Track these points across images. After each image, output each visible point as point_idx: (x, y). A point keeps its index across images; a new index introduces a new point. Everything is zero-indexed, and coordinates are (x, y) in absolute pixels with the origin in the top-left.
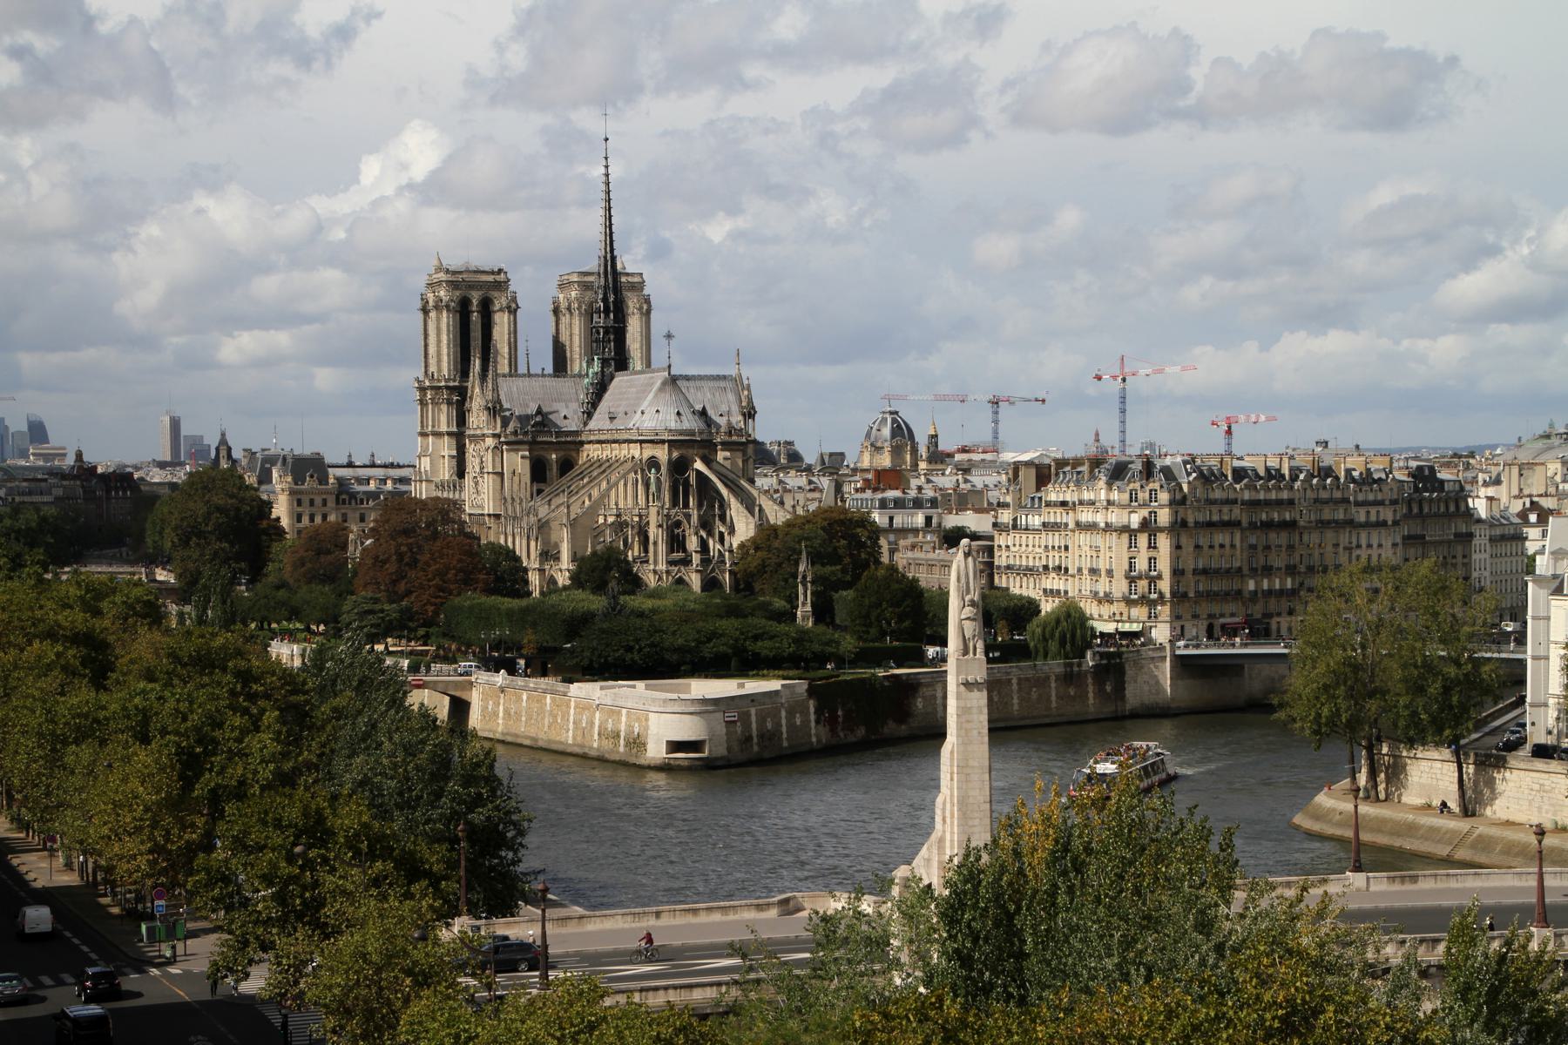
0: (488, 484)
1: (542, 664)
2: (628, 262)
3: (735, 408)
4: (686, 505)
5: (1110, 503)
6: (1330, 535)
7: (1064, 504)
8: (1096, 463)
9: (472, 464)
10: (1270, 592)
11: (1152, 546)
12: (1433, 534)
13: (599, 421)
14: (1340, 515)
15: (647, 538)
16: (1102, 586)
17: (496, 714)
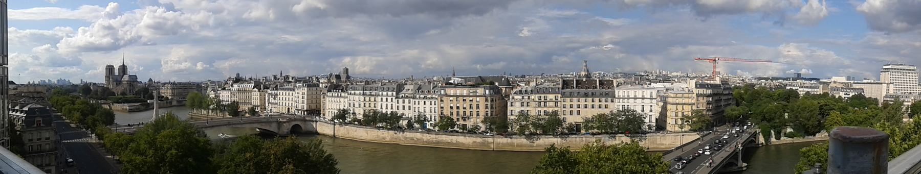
1: (118, 102)
2: (125, 64)
8: (169, 83)
12: (199, 89)
13: (123, 79)
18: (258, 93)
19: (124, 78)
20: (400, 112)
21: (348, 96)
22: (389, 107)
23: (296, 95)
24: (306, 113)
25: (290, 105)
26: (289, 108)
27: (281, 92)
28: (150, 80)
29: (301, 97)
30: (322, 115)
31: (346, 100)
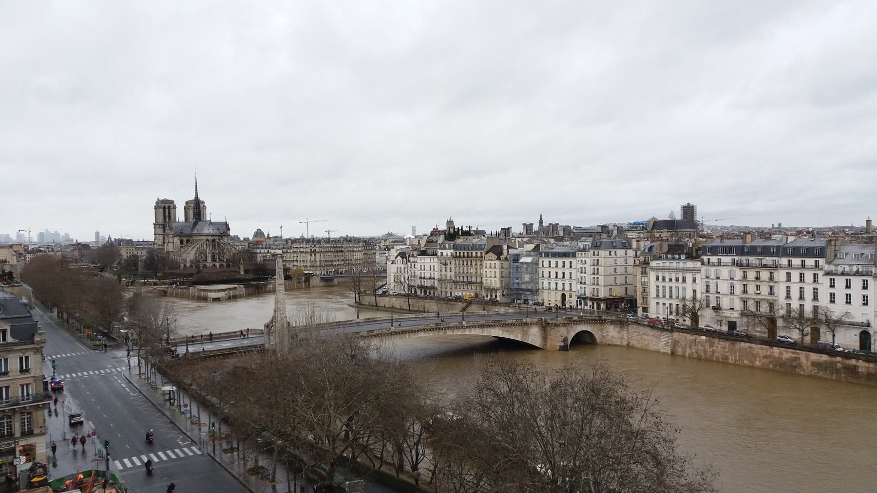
0: (171, 245)
2: (201, 198)
3: (225, 229)
4: (215, 249)
5: (306, 247)
6: (350, 253)
7: (297, 248)
9: (166, 241)
10: (338, 265)
11: (315, 256)
13: (195, 232)
14: (352, 249)
15: (206, 256)
16: (305, 264)
17: (173, 294)
18: (498, 263)
19: (197, 227)
20: (838, 310)
21: (703, 268)
22: (808, 294)
23: (579, 266)
24: (602, 306)
25: (567, 288)
26: (563, 296)
27: (546, 260)
28: (259, 233)
29: (590, 270)
30: (640, 311)
31: (698, 276)
